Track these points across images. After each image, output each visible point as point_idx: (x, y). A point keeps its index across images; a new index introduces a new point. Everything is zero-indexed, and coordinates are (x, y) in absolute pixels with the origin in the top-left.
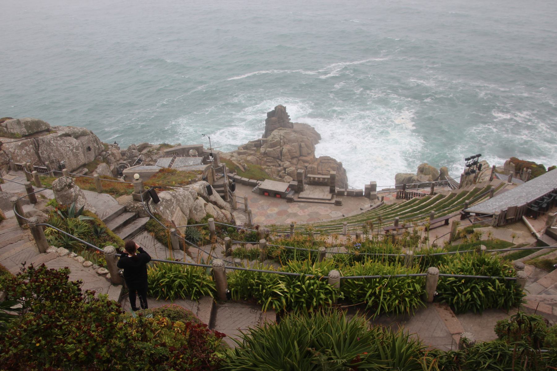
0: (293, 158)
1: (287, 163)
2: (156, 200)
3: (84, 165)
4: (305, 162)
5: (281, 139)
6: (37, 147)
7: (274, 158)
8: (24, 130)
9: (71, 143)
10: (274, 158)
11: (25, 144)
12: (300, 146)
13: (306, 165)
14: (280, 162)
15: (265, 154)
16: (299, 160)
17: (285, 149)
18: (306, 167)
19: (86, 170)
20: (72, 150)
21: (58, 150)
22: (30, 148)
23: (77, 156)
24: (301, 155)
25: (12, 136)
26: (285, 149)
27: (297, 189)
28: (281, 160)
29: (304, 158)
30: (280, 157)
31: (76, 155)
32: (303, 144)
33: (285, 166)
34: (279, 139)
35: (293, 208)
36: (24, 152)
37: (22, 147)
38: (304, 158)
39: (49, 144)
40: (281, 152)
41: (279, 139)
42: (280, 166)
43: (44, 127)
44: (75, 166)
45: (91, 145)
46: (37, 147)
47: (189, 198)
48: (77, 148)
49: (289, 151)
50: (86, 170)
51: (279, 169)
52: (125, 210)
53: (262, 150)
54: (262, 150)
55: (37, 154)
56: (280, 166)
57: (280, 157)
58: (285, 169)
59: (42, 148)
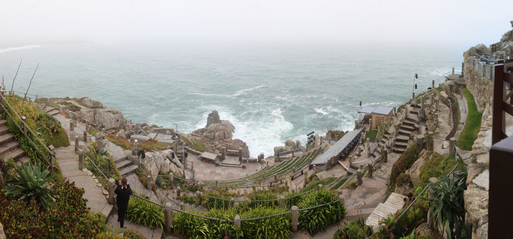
0: (220, 140)
1: (217, 142)
2: (144, 157)
3: (114, 128)
4: (226, 142)
6: (95, 114)
8: (92, 104)
11: (90, 111)
13: (227, 143)
15: (206, 136)
19: (114, 131)
21: (104, 118)
22: (92, 114)
24: (225, 138)
25: (86, 106)
27: (221, 158)
29: (226, 140)
30: (213, 139)
31: (111, 122)
35: (219, 170)
36: (89, 115)
37: (88, 112)
38: (226, 140)
39: (100, 114)
40: (214, 136)
42: (213, 144)
43: (100, 106)
44: (109, 128)
45: (119, 119)
46: (95, 114)
47: (161, 159)
50: (114, 131)
51: (213, 145)
52: (127, 158)
53: (205, 134)
54: (205, 134)
55: (94, 117)
56: (213, 144)
57: (213, 139)
58: (216, 146)
59: (97, 115)
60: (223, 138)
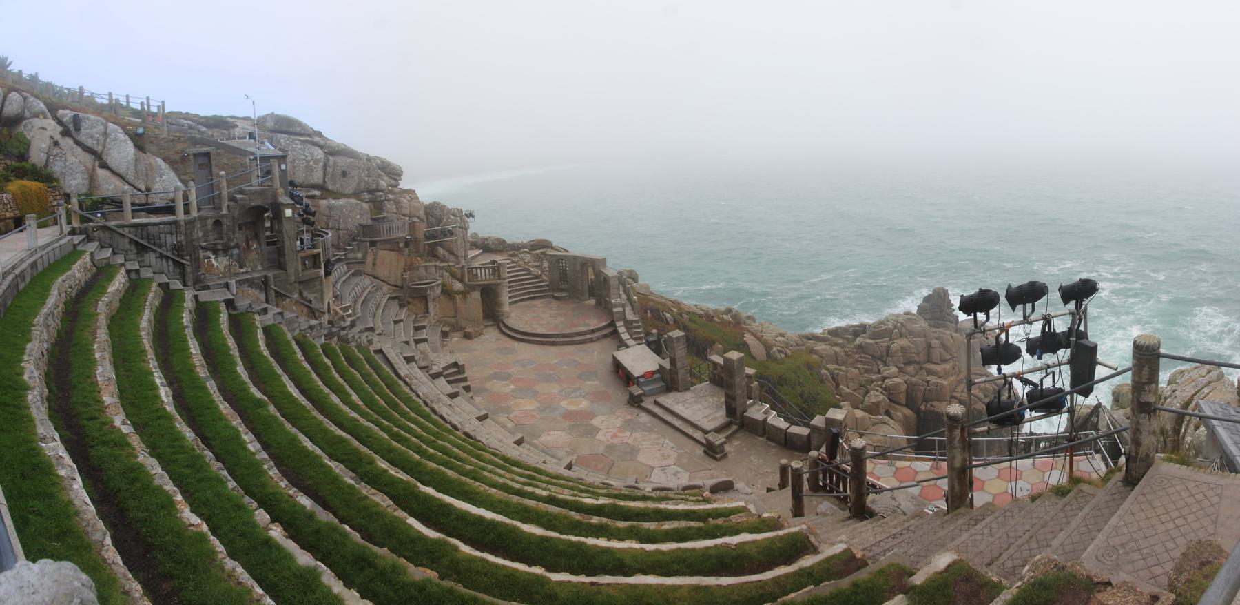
1: (893, 369)
4: (929, 372)
5: (895, 327)
7: (873, 356)
9: (312, 154)
10: (873, 356)
12: (929, 346)
13: (929, 378)
14: (881, 367)
15: (860, 347)
16: (922, 368)
17: (896, 345)
18: (928, 382)
20: (308, 162)
23: (312, 170)
24: (929, 361)
26: (896, 345)
28: (885, 364)
29: (932, 366)
30: (885, 357)
31: (310, 170)
32: (935, 343)
33: (885, 374)
34: (891, 327)
38: (932, 366)
40: (889, 347)
41: (891, 327)
42: (879, 372)
48: (316, 162)
49: (903, 348)
53: (859, 341)
54: (859, 341)
56: (879, 372)
57: (885, 357)
58: (884, 378)
60: (923, 357)
